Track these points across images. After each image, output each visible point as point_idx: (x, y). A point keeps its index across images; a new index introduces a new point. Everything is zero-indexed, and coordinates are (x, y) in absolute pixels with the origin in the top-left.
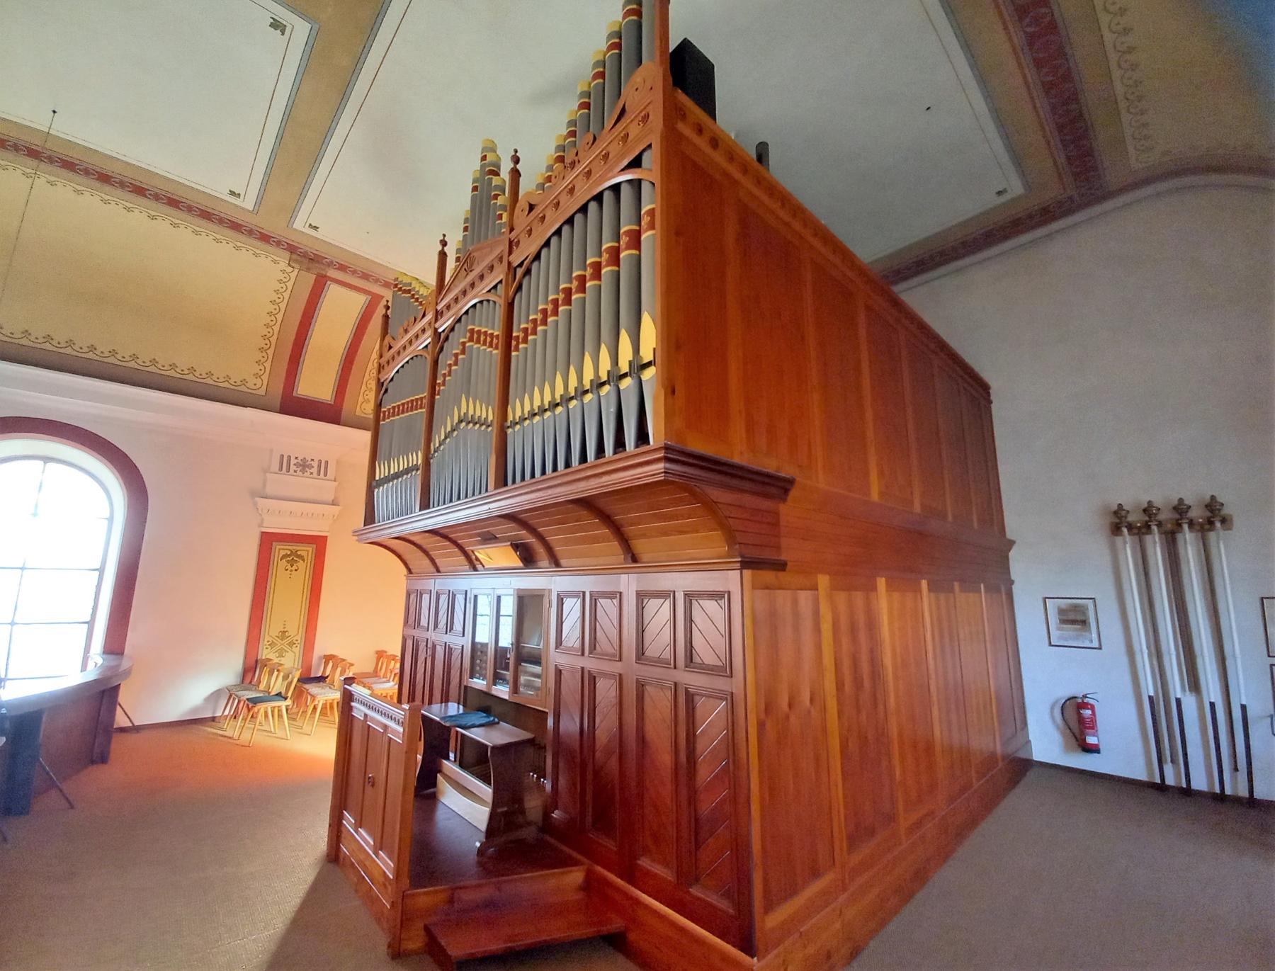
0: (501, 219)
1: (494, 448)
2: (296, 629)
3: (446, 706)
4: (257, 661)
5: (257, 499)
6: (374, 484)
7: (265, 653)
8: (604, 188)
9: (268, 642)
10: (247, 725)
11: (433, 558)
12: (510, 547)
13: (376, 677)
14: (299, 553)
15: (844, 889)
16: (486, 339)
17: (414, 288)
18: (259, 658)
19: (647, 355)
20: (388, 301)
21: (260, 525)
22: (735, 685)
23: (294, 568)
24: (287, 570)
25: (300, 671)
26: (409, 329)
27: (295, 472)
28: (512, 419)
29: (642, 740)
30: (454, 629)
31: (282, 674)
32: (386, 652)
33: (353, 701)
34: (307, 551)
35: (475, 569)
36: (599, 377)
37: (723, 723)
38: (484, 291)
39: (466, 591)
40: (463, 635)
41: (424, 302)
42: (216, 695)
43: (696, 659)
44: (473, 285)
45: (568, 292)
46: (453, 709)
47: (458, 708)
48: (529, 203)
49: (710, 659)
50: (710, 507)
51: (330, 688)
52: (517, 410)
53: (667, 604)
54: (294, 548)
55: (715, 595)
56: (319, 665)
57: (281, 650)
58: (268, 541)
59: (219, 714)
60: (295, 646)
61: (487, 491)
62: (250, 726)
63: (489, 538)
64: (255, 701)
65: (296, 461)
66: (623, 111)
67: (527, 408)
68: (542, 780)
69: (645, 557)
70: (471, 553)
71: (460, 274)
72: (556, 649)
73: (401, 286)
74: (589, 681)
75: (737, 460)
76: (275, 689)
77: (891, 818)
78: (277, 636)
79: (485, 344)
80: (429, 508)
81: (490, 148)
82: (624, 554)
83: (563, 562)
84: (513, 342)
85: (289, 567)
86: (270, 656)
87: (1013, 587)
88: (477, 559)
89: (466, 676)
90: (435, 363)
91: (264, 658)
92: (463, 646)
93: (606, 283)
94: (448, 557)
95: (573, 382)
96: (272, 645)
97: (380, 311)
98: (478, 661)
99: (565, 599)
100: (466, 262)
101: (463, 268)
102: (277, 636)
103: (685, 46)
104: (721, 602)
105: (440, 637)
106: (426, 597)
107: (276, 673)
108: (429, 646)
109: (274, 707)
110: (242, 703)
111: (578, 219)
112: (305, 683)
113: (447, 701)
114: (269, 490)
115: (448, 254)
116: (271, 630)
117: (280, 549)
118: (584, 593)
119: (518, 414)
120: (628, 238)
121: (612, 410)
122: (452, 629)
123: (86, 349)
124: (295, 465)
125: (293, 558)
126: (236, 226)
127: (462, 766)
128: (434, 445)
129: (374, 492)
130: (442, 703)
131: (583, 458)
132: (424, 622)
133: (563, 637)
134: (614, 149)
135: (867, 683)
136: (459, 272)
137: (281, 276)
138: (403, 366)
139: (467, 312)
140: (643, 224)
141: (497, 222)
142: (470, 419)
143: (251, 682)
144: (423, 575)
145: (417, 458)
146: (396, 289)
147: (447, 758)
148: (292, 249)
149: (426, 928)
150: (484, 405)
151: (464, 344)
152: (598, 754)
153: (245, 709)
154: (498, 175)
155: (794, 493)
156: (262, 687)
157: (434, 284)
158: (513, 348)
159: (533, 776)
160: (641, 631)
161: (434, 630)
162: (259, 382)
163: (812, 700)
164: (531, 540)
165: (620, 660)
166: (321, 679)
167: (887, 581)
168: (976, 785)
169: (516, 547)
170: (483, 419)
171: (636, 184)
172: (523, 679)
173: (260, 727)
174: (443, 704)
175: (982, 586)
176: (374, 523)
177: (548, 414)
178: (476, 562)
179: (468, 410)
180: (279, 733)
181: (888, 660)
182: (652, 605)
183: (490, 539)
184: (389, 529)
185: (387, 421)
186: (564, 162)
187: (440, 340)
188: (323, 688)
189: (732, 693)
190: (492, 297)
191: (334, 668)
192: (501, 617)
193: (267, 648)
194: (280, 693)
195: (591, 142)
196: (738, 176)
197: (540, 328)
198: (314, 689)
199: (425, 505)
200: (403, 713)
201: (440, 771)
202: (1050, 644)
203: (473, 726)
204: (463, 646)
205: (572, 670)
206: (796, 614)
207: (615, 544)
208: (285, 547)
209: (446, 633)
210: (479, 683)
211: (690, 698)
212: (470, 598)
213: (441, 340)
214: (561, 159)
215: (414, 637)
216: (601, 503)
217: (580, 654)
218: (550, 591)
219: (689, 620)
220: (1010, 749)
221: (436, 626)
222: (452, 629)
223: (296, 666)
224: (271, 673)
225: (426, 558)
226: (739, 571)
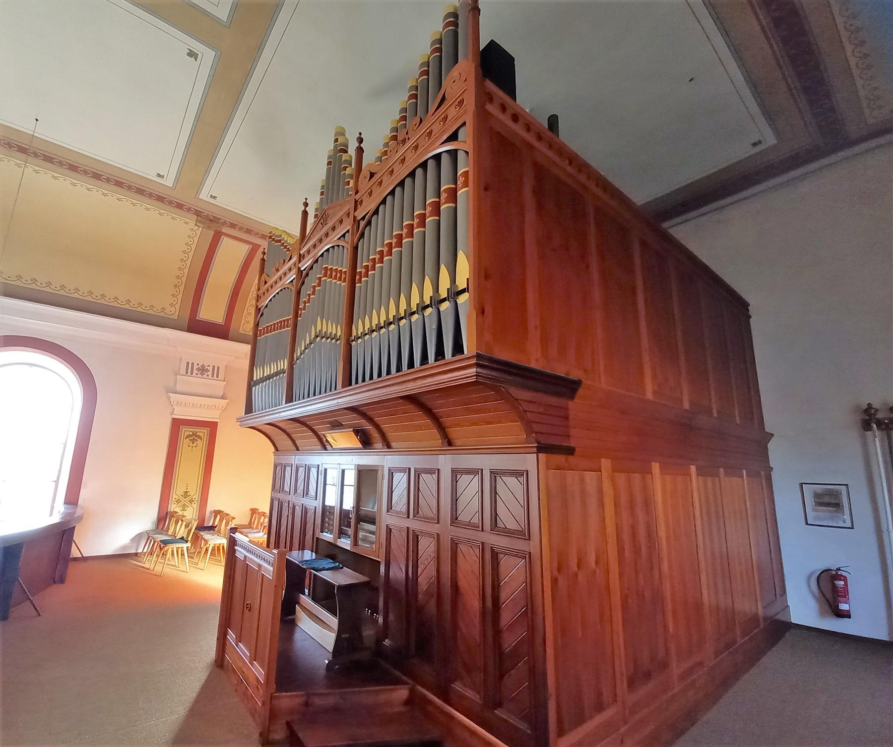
0: (349, 185)
2: (195, 492)
3: (303, 553)
4: (167, 513)
6: (252, 383)
7: (173, 507)
8: (427, 158)
9: (175, 499)
10: (159, 560)
12: (352, 432)
13: (251, 528)
14: (198, 434)
15: (625, 723)
17: (284, 239)
18: (169, 510)
19: (461, 284)
20: (264, 249)
21: (172, 413)
22: (533, 546)
23: (195, 444)
24: (189, 446)
25: (198, 521)
27: (197, 374)
28: (355, 335)
29: (455, 587)
30: (309, 494)
31: (184, 523)
32: (258, 510)
33: (236, 545)
34: (204, 432)
35: (325, 449)
36: (424, 302)
37: (522, 578)
38: (335, 239)
39: (319, 465)
40: (316, 499)
41: (291, 249)
42: (139, 537)
43: (500, 524)
44: (327, 235)
45: (400, 237)
46: (308, 555)
47: (312, 554)
48: (370, 172)
49: (511, 525)
50: (514, 403)
51: (218, 535)
52: (359, 328)
53: (477, 479)
54: (195, 430)
55: (517, 474)
57: (184, 505)
58: (177, 424)
59: (140, 551)
60: (194, 502)
61: (336, 389)
62: (162, 561)
63: (337, 426)
64: (166, 543)
65: (198, 366)
66: (443, 99)
67: (367, 326)
68: (375, 615)
69: (457, 442)
70: (323, 437)
72: (387, 512)
73: (274, 237)
74: (413, 538)
75: (533, 365)
76: (179, 535)
77: (664, 665)
78: (181, 495)
79: (335, 278)
80: (292, 402)
81: (341, 133)
82: (442, 439)
83: (393, 444)
86: (177, 510)
87: (772, 473)
88: (327, 441)
89: (318, 530)
91: (172, 511)
92: (316, 507)
93: (429, 229)
94: (305, 438)
95: (403, 306)
96: (178, 501)
97: (259, 256)
98: (327, 520)
99: (394, 474)
100: (322, 218)
101: (320, 222)
102: (181, 495)
103: (492, 45)
104: (521, 479)
105: (299, 501)
106: (288, 469)
107: (180, 522)
108: (290, 506)
109: (179, 548)
110: (156, 543)
111: (408, 181)
112: (201, 531)
113: (303, 549)
114: (179, 388)
115: (309, 212)
116: (177, 491)
117: (185, 431)
118: (409, 469)
119: (361, 330)
120: (446, 195)
121: (434, 327)
122: (307, 494)
123: (59, 288)
124: (197, 369)
125: (194, 437)
126: (160, 199)
127: (314, 599)
128: (297, 355)
129: (252, 389)
130: (299, 550)
131: (411, 365)
132: (287, 489)
133: (393, 504)
134: (436, 128)
135: (644, 551)
137: (190, 233)
138: (274, 296)
139: (322, 255)
140: (458, 183)
141: (346, 187)
143: (162, 529)
144: (286, 451)
145: (284, 364)
146: (271, 240)
147: (304, 594)
148: (198, 213)
149: (288, 724)
150: (334, 324)
151: (320, 278)
152: (420, 596)
153: (158, 549)
154: (346, 152)
155: (581, 392)
156: (170, 533)
157: (299, 235)
158: (357, 281)
159: (368, 611)
160: (455, 500)
161: (294, 494)
163: (597, 563)
164: (369, 427)
165: (438, 522)
166: (212, 528)
167: (660, 467)
168: (740, 641)
169: (358, 432)
171: (453, 154)
172: (361, 534)
173: (168, 562)
174: (301, 551)
175: (744, 471)
176: (252, 413)
178: (326, 444)
180: (182, 568)
181: (662, 533)
182: (464, 480)
183: (339, 426)
184: (262, 419)
186: (397, 141)
187: (302, 276)
188: (213, 535)
189: (530, 553)
190: (341, 243)
191: (221, 520)
192: (345, 487)
193: (174, 504)
194: (183, 537)
195: (418, 124)
196: (535, 143)
198: (206, 536)
199: (290, 399)
200: (273, 557)
201: (298, 603)
202: (807, 524)
203: (323, 569)
205: (400, 530)
206: (583, 491)
207: (435, 432)
208: (189, 429)
209: (303, 497)
210: (328, 536)
211: (495, 555)
212: (321, 471)
214: (395, 138)
216: (424, 399)
217: (406, 516)
219: (494, 493)
220: (771, 612)
222: (308, 494)
223: (194, 518)
224: (177, 522)
225: (289, 440)
226: (536, 454)
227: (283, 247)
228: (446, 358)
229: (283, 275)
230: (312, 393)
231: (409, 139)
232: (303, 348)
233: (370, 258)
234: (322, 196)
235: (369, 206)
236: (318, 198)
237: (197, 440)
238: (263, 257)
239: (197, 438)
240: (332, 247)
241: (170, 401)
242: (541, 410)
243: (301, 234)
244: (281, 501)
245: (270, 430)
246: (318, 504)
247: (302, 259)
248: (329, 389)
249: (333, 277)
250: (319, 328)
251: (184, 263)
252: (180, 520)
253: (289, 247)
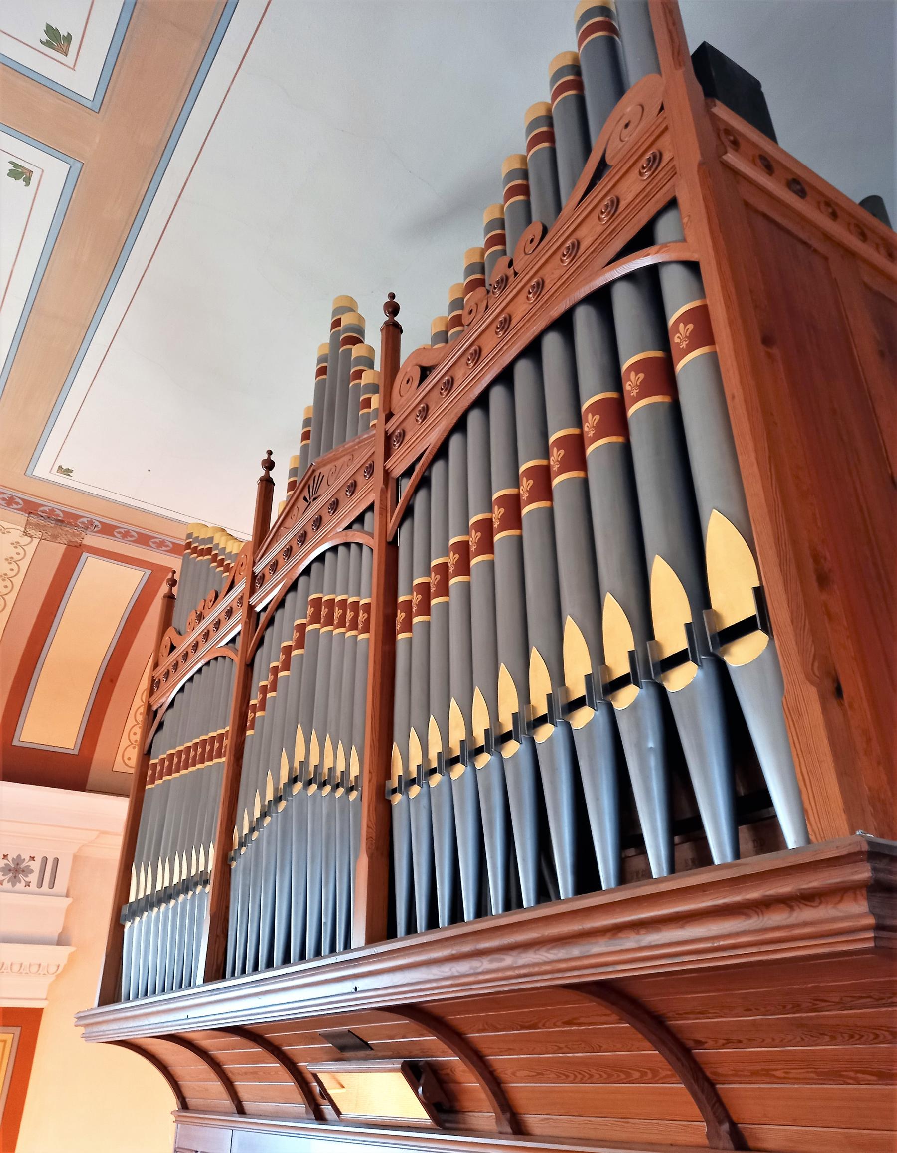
26: (205, 612)
41: (232, 565)
97: (164, 589)
190: (356, 536)
227: (215, 564)
233: (433, 563)
253: (229, 562)
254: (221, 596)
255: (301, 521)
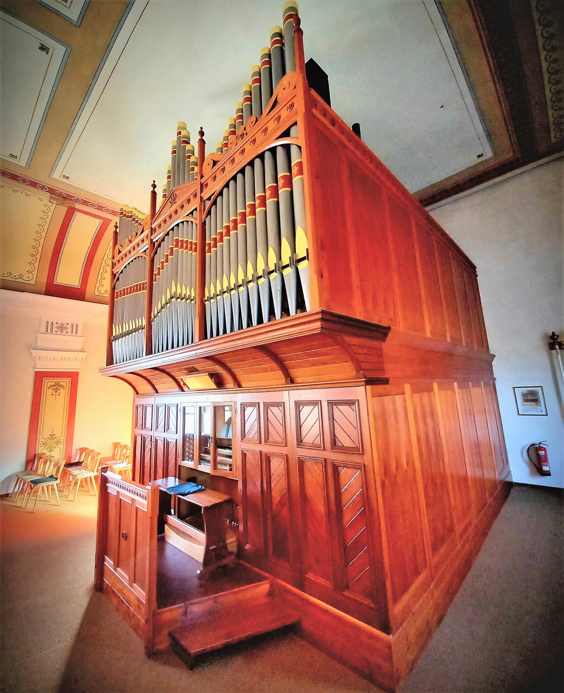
1: (197, 315)
4: (35, 455)
5: (31, 350)
6: (112, 338)
7: (40, 450)
10: (30, 498)
11: (153, 384)
12: (208, 376)
14: (60, 384)
16: (189, 246)
18: (36, 453)
20: (116, 223)
22: (367, 459)
23: (58, 393)
25: (65, 460)
29: (304, 496)
30: (170, 428)
31: (53, 463)
34: (65, 382)
37: (358, 484)
39: (177, 404)
40: (177, 433)
42: (9, 478)
43: (339, 444)
44: (176, 212)
46: (172, 482)
48: (213, 160)
49: (347, 443)
52: (210, 291)
54: (58, 380)
55: (350, 403)
56: (76, 455)
59: (11, 491)
60: (60, 443)
61: (192, 342)
62: (33, 498)
63: (192, 371)
64: (36, 482)
67: (219, 288)
69: (299, 380)
70: (180, 381)
71: (167, 205)
74: (266, 460)
76: (47, 474)
79: (186, 248)
80: (152, 354)
83: (243, 384)
84: (206, 246)
85: (54, 393)
88: (185, 384)
90: (152, 261)
92: (176, 440)
94: (164, 383)
96: (45, 444)
98: (187, 449)
99: (245, 408)
100: (170, 197)
101: (169, 202)
104: (353, 407)
105: (160, 435)
106: (149, 410)
107: (49, 463)
108: (152, 441)
113: (167, 477)
116: (44, 434)
117: (48, 382)
119: (213, 292)
125: (57, 387)
127: (180, 517)
130: (163, 478)
132: (148, 425)
133: (246, 433)
136: (166, 203)
138: (129, 264)
139: (172, 229)
141: (191, 172)
142: (178, 296)
143: (31, 469)
144: (145, 395)
147: (171, 514)
151: (172, 248)
156: (40, 471)
158: (206, 251)
160: (299, 427)
161: (156, 430)
162: (31, 276)
165: (286, 446)
166: (78, 464)
169: (212, 375)
170: (188, 296)
172: (219, 458)
173: (40, 499)
174: (165, 479)
177: (233, 292)
178: (183, 386)
179: (191, 294)
184: (123, 369)
185: (119, 298)
187: (155, 247)
189: (365, 464)
191: (87, 456)
193: (41, 446)
197: (225, 238)
199: (149, 351)
204: (176, 440)
207: (280, 373)
208: (52, 380)
209: (165, 432)
210: (189, 464)
211: (336, 469)
213: (155, 247)
214: (233, 133)
215: (142, 435)
217: (258, 443)
218: (235, 402)
219: (332, 419)
221: (157, 428)
224: (45, 463)
227: (134, 222)
228: (291, 315)
229: (136, 246)
230: (172, 346)
231: (247, 134)
232: (160, 308)
234: (170, 180)
235: (214, 187)
236: (165, 181)
237: (59, 389)
238: (116, 230)
239: (60, 388)
240: (181, 222)
241: (32, 357)
242: (365, 351)
243: (151, 212)
244: (144, 436)
245: (131, 378)
246: (179, 437)
247: (154, 232)
248: (189, 340)
249: (184, 247)
250: (174, 290)
251: (39, 235)
252: (48, 461)
253: (140, 222)
254: (138, 235)
255: (170, 210)
